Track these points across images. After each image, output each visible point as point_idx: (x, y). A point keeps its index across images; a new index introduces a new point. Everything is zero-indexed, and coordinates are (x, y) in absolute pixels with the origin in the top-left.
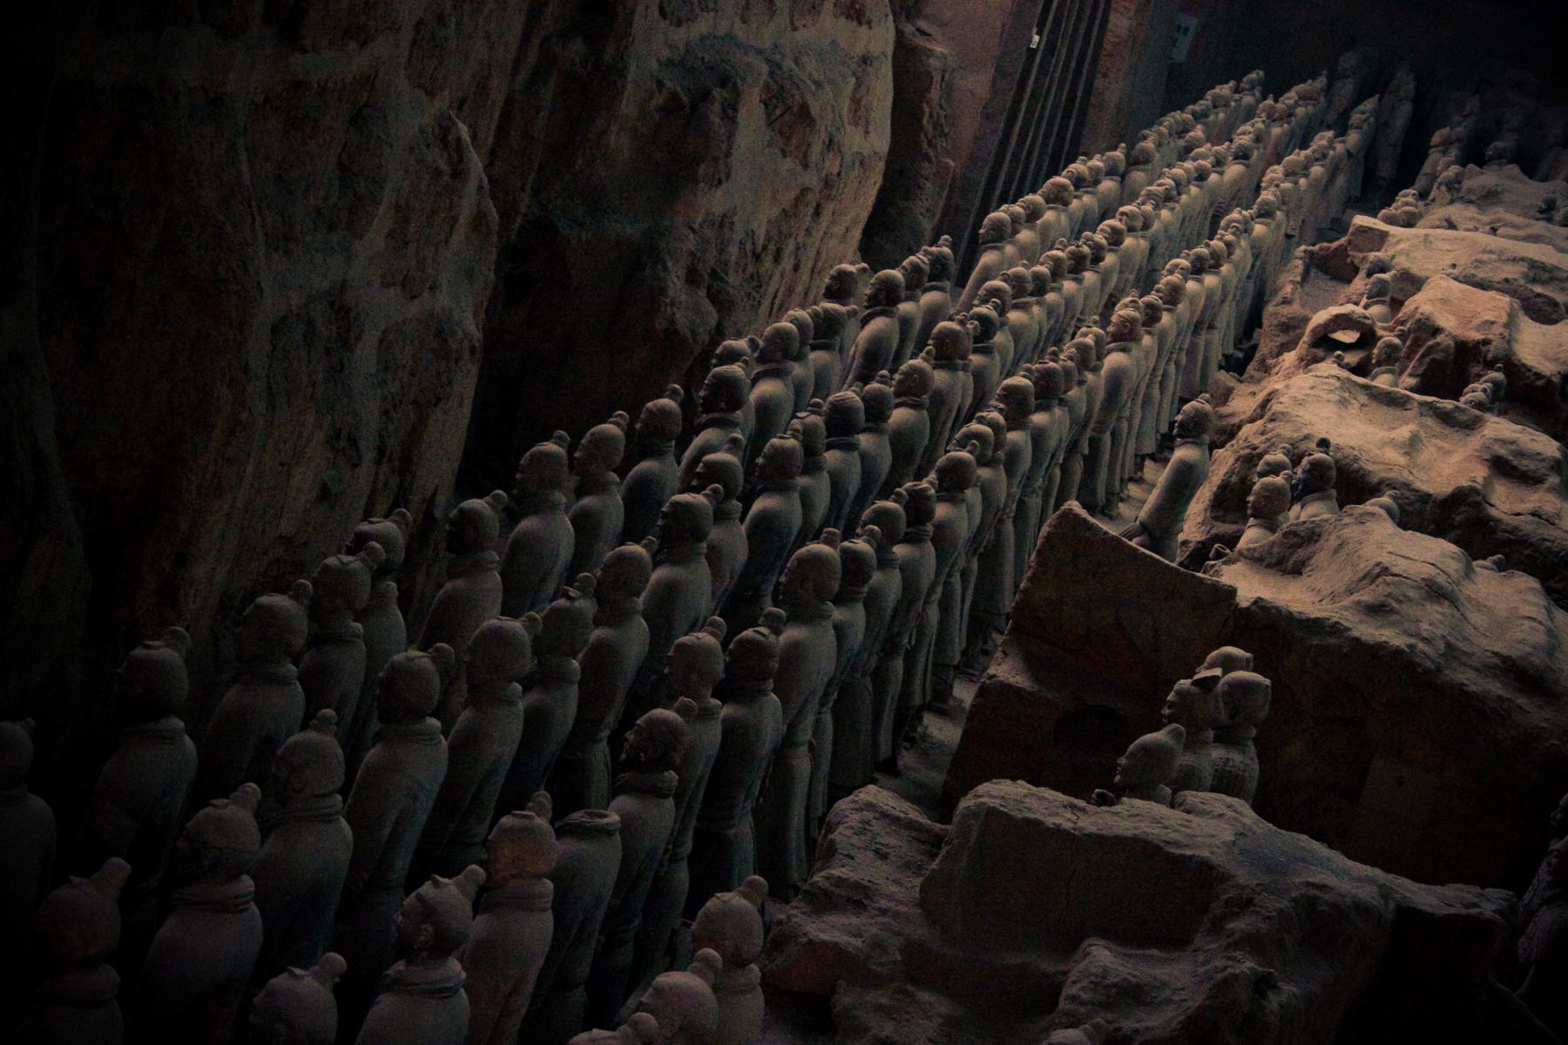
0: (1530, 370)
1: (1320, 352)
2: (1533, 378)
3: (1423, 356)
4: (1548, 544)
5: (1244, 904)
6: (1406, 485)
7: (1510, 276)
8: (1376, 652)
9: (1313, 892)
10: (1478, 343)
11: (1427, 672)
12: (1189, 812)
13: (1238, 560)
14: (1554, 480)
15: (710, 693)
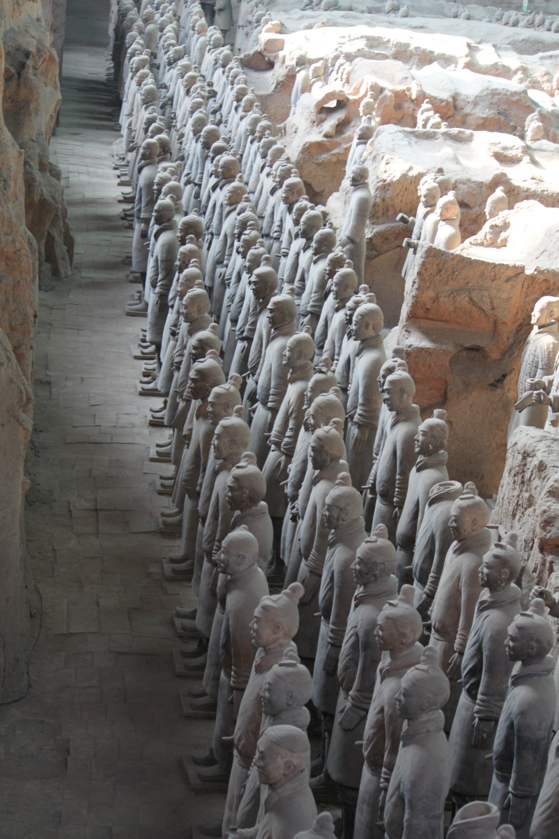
0: (436, 99)
1: (323, 116)
2: (439, 102)
4: (546, 193)
6: (469, 180)
7: (360, 48)
10: (404, 91)
15: (411, 401)
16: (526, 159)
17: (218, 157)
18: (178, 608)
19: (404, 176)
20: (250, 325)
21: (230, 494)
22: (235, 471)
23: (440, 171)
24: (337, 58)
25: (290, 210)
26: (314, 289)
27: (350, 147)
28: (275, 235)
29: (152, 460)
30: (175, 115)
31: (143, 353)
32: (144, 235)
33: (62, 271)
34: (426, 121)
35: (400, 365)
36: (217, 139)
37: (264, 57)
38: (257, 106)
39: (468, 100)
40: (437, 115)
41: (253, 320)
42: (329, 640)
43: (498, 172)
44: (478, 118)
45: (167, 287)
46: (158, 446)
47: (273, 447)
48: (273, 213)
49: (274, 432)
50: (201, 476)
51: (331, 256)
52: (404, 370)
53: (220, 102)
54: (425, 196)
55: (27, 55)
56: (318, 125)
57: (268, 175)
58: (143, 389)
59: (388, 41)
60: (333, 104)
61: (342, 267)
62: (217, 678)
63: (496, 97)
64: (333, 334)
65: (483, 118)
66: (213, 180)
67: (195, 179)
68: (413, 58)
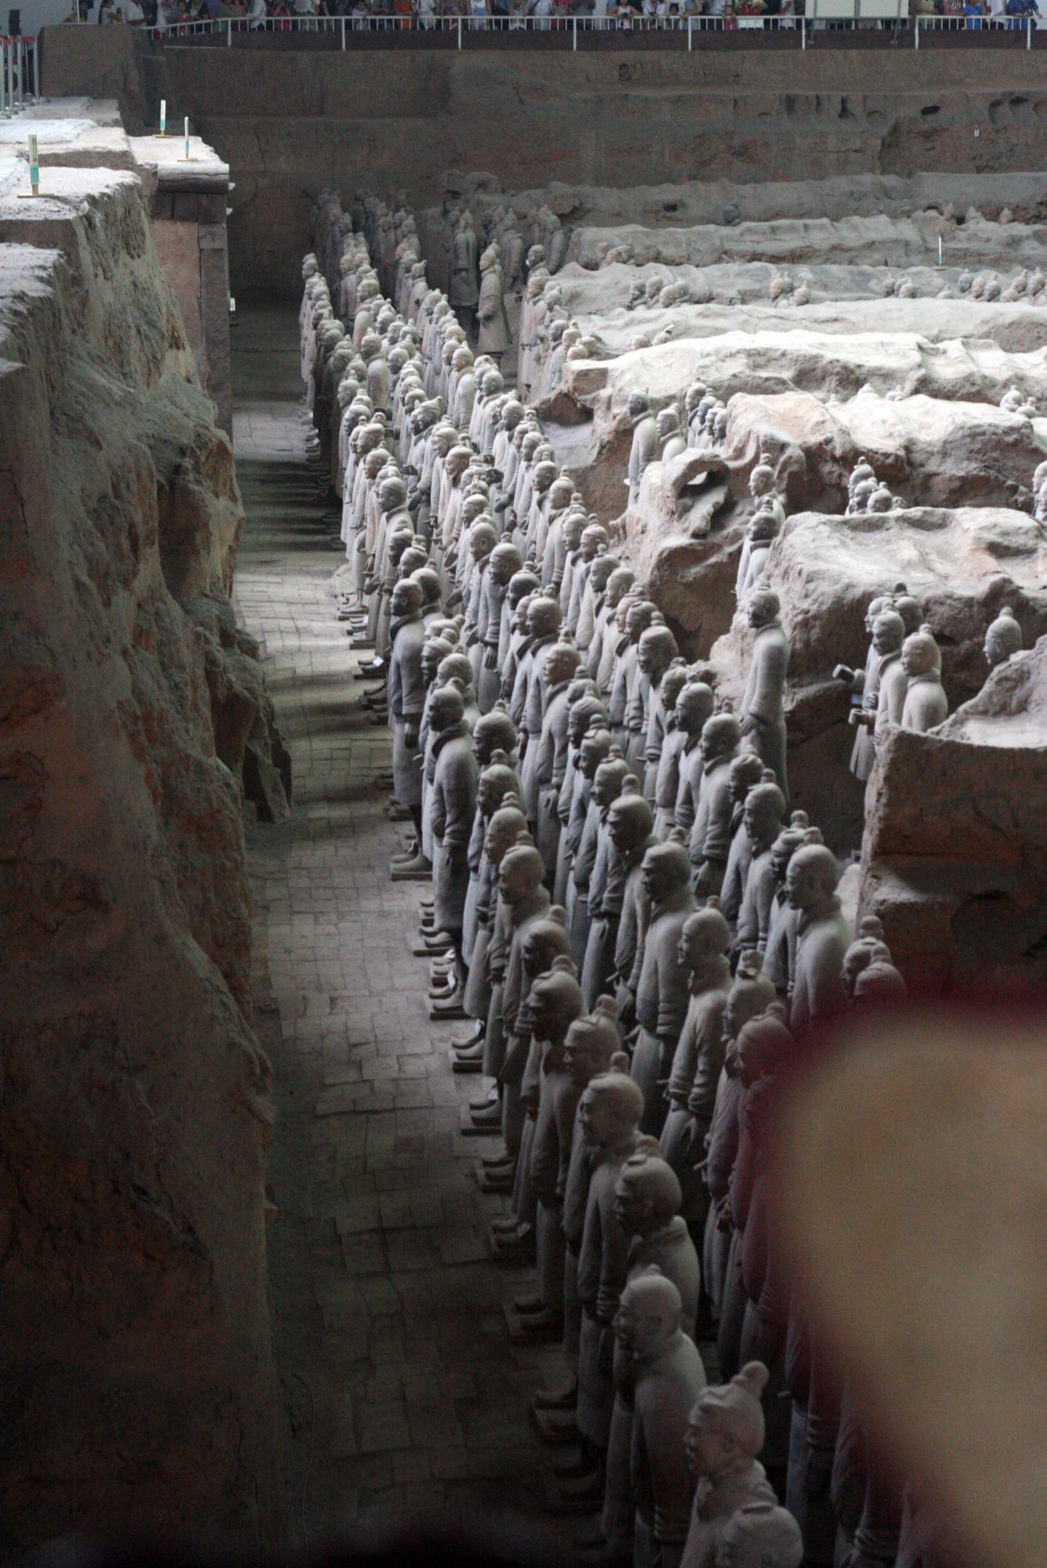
0: (876, 453)
1: (687, 501)
2: (882, 458)
3: (781, 472)
6: (950, 597)
7: (735, 371)
10: (821, 444)
13: (967, 719)
17: (523, 601)
18: (540, 1393)
19: (839, 601)
20: (610, 892)
21: (621, 1209)
22: (628, 1171)
23: (901, 588)
24: (700, 394)
25: (655, 682)
26: (711, 818)
27: (739, 551)
28: (632, 724)
29: (466, 1133)
30: (436, 521)
31: (428, 945)
32: (412, 743)
33: (275, 810)
34: (865, 495)
35: (878, 952)
36: (517, 567)
37: (574, 402)
38: (576, 499)
39: (929, 449)
40: (882, 484)
41: (615, 882)
42: (809, 1440)
43: (997, 578)
44: (952, 478)
45: (462, 837)
46: (473, 1107)
47: (673, 1103)
48: (624, 688)
49: (673, 1079)
50: (561, 1169)
51: (735, 762)
52: (885, 960)
53: (509, 489)
54: (879, 636)
55: (182, 452)
56: (680, 517)
57: (610, 620)
58: (435, 1008)
59: (784, 354)
60: (700, 479)
61: (756, 781)
62: (628, 1521)
63: (980, 438)
64: (753, 895)
66: (517, 640)
67: (484, 634)
68: (828, 380)
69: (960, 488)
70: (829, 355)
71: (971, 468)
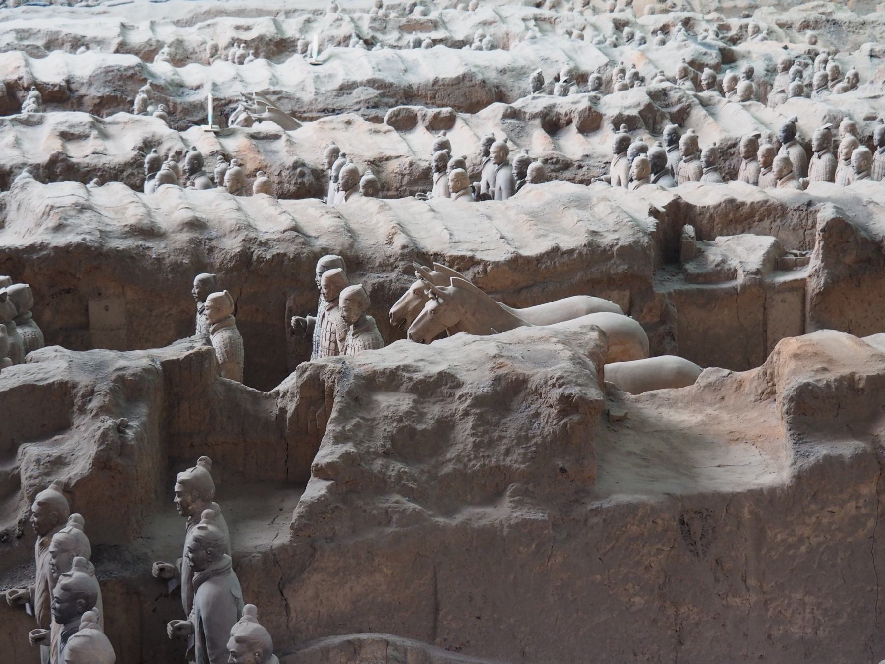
2: (51, 87)
5: (91, 393)
7: (9, 41)
8: (66, 251)
9: (120, 373)
11: (97, 249)
12: (38, 362)
14: (95, 133)
16: (95, 133)
39: (82, 81)
44: (93, 99)
59: (39, 31)
63: (110, 74)
65: (99, 97)
68: (65, 45)
69: (100, 102)
70: (65, 31)
71: (106, 91)
